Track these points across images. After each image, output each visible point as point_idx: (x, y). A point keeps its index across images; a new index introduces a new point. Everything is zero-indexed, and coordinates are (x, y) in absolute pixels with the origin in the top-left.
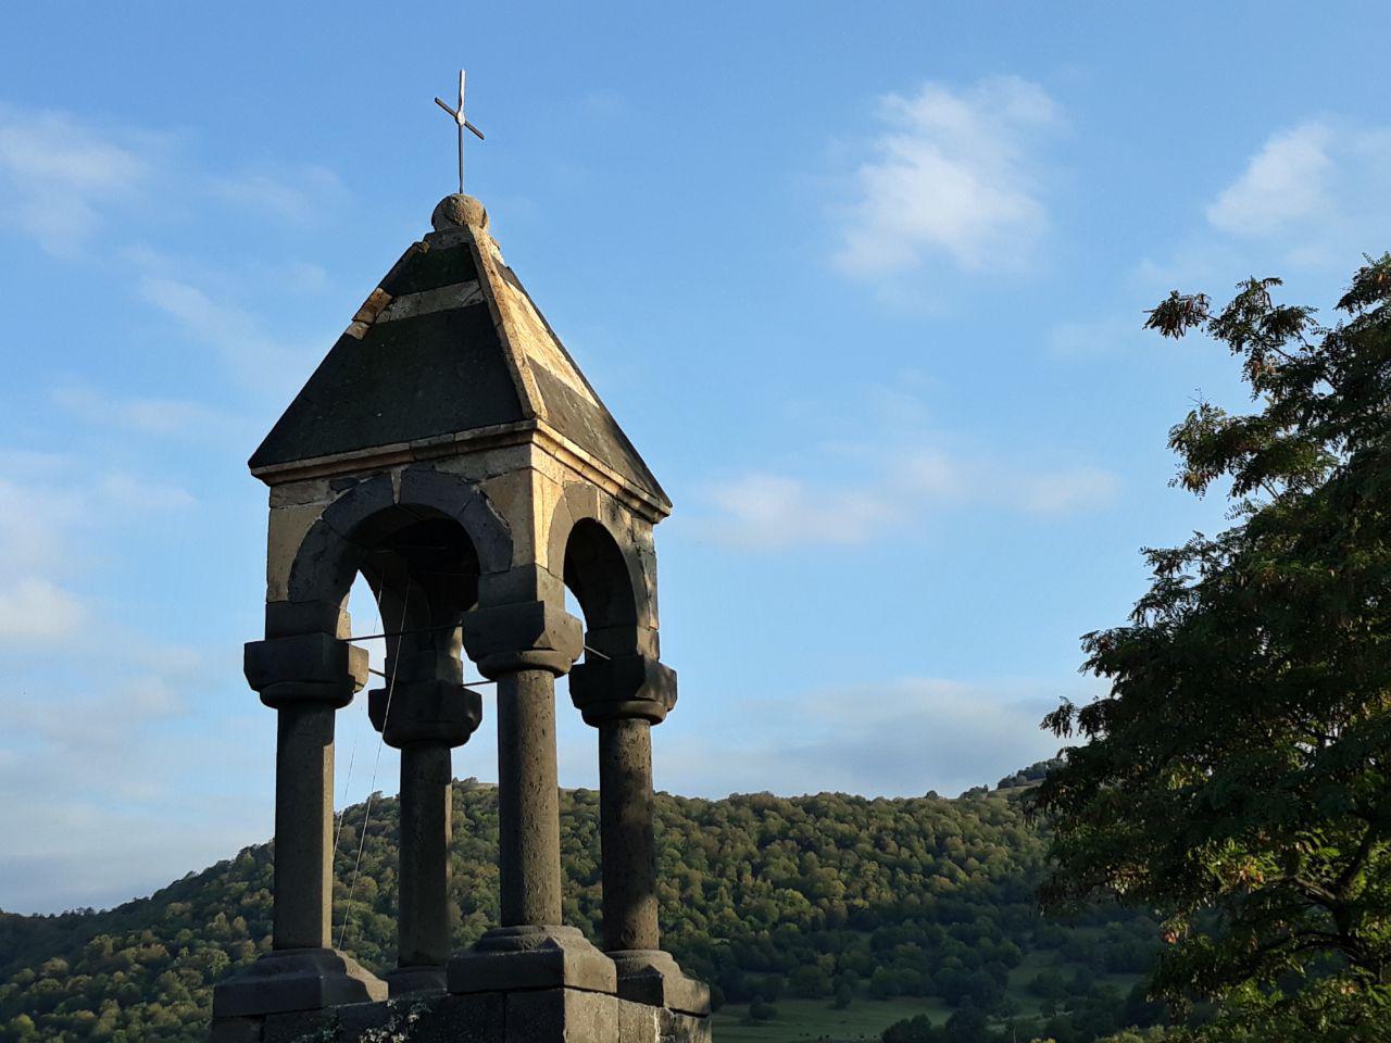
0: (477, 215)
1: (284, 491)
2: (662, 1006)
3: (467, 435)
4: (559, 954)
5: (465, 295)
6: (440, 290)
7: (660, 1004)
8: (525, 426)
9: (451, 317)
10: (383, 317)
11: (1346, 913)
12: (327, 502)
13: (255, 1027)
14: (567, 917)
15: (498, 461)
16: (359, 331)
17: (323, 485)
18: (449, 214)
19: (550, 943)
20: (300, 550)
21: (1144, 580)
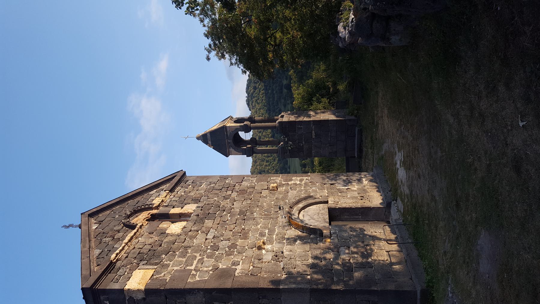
0: (199, 135)
1: (230, 154)
2: (284, 115)
3: (225, 133)
4: (279, 122)
5: (209, 135)
6: (208, 138)
7: (284, 115)
8: (225, 126)
9: (211, 137)
10: (211, 144)
11: (276, 45)
12: (232, 149)
13: (285, 154)
14: (276, 122)
15: (228, 129)
16: (212, 147)
17: (230, 149)
18: (198, 138)
19: (278, 123)
20: (237, 151)
21: (235, 67)
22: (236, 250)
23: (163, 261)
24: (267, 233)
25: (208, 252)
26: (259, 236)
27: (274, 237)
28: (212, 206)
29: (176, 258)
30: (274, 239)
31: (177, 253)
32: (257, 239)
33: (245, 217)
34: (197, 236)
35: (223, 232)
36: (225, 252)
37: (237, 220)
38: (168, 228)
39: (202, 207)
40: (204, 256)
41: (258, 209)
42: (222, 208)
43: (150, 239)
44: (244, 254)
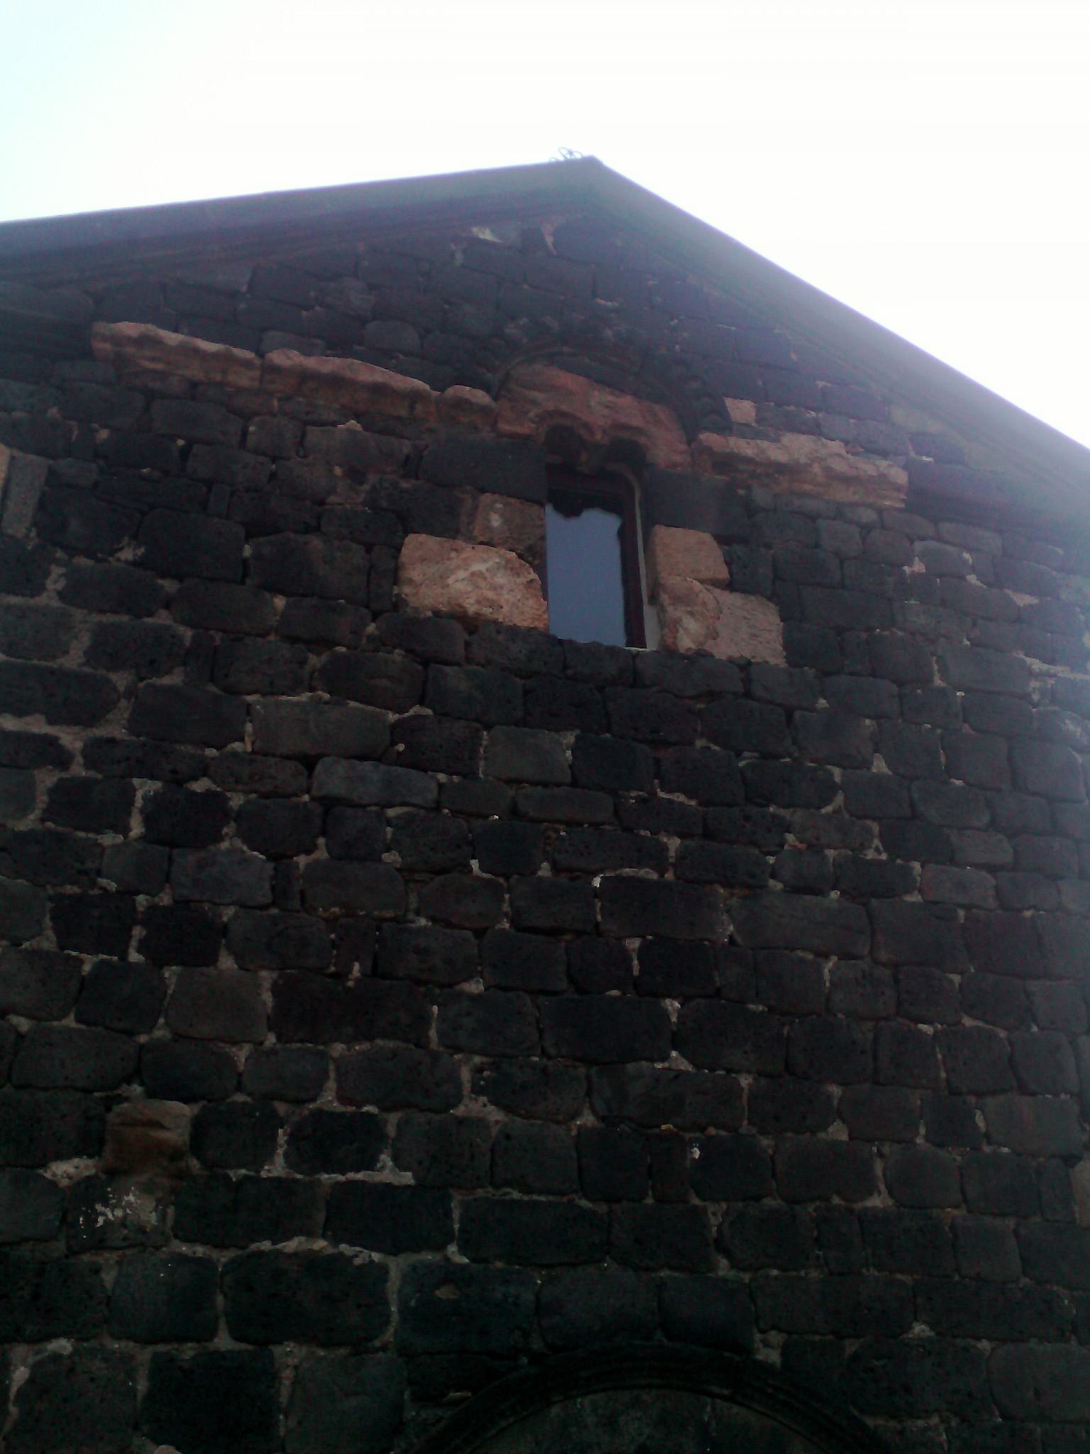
22: (134, 957)
23: (83, 561)
24: (360, 1176)
25: (136, 781)
26: (320, 1114)
27: (292, 1245)
28: (766, 756)
29: (95, 618)
30: (266, 1245)
31: (163, 618)
32: (281, 1108)
33: (615, 993)
34: (352, 704)
35: (391, 858)
36: (113, 886)
37: (578, 933)
38: (470, 539)
39: (748, 694)
40: (90, 763)
41: (745, 1081)
42: (747, 818)
43: (338, 471)
44: (70, 1022)
